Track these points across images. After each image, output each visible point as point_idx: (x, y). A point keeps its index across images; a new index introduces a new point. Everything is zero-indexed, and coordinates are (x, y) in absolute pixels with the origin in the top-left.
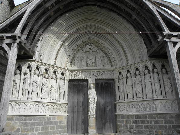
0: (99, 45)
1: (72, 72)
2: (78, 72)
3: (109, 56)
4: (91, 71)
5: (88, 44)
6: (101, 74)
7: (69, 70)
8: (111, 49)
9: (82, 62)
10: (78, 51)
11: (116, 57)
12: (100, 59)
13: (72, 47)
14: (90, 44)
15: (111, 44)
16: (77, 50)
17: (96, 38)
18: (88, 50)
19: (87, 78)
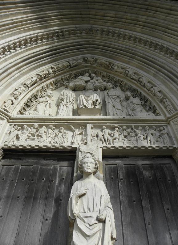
0: (111, 75)
1: (22, 128)
2: (41, 126)
3: (143, 93)
4: (89, 126)
5: (82, 74)
6: (125, 133)
7: (10, 120)
8: (146, 77)
9: (61, 106)
10: (54, 86)
11: (166, 90)
12: (118, 101)
13: (39, 69)
14: (87, 74)
15: (147, 63)
16: (51, 81)
17: (103, 60)
18: (82, 83)
19: (74, 146)
